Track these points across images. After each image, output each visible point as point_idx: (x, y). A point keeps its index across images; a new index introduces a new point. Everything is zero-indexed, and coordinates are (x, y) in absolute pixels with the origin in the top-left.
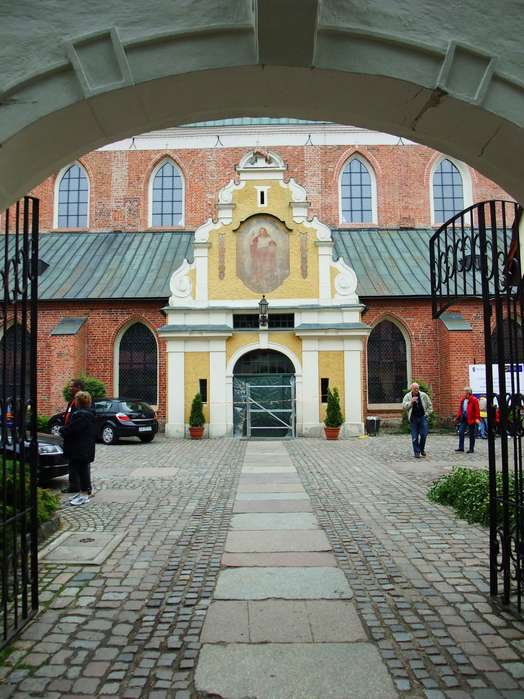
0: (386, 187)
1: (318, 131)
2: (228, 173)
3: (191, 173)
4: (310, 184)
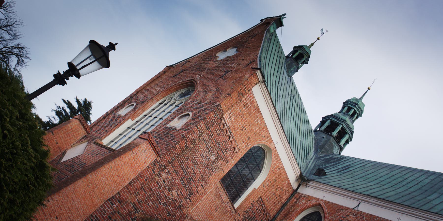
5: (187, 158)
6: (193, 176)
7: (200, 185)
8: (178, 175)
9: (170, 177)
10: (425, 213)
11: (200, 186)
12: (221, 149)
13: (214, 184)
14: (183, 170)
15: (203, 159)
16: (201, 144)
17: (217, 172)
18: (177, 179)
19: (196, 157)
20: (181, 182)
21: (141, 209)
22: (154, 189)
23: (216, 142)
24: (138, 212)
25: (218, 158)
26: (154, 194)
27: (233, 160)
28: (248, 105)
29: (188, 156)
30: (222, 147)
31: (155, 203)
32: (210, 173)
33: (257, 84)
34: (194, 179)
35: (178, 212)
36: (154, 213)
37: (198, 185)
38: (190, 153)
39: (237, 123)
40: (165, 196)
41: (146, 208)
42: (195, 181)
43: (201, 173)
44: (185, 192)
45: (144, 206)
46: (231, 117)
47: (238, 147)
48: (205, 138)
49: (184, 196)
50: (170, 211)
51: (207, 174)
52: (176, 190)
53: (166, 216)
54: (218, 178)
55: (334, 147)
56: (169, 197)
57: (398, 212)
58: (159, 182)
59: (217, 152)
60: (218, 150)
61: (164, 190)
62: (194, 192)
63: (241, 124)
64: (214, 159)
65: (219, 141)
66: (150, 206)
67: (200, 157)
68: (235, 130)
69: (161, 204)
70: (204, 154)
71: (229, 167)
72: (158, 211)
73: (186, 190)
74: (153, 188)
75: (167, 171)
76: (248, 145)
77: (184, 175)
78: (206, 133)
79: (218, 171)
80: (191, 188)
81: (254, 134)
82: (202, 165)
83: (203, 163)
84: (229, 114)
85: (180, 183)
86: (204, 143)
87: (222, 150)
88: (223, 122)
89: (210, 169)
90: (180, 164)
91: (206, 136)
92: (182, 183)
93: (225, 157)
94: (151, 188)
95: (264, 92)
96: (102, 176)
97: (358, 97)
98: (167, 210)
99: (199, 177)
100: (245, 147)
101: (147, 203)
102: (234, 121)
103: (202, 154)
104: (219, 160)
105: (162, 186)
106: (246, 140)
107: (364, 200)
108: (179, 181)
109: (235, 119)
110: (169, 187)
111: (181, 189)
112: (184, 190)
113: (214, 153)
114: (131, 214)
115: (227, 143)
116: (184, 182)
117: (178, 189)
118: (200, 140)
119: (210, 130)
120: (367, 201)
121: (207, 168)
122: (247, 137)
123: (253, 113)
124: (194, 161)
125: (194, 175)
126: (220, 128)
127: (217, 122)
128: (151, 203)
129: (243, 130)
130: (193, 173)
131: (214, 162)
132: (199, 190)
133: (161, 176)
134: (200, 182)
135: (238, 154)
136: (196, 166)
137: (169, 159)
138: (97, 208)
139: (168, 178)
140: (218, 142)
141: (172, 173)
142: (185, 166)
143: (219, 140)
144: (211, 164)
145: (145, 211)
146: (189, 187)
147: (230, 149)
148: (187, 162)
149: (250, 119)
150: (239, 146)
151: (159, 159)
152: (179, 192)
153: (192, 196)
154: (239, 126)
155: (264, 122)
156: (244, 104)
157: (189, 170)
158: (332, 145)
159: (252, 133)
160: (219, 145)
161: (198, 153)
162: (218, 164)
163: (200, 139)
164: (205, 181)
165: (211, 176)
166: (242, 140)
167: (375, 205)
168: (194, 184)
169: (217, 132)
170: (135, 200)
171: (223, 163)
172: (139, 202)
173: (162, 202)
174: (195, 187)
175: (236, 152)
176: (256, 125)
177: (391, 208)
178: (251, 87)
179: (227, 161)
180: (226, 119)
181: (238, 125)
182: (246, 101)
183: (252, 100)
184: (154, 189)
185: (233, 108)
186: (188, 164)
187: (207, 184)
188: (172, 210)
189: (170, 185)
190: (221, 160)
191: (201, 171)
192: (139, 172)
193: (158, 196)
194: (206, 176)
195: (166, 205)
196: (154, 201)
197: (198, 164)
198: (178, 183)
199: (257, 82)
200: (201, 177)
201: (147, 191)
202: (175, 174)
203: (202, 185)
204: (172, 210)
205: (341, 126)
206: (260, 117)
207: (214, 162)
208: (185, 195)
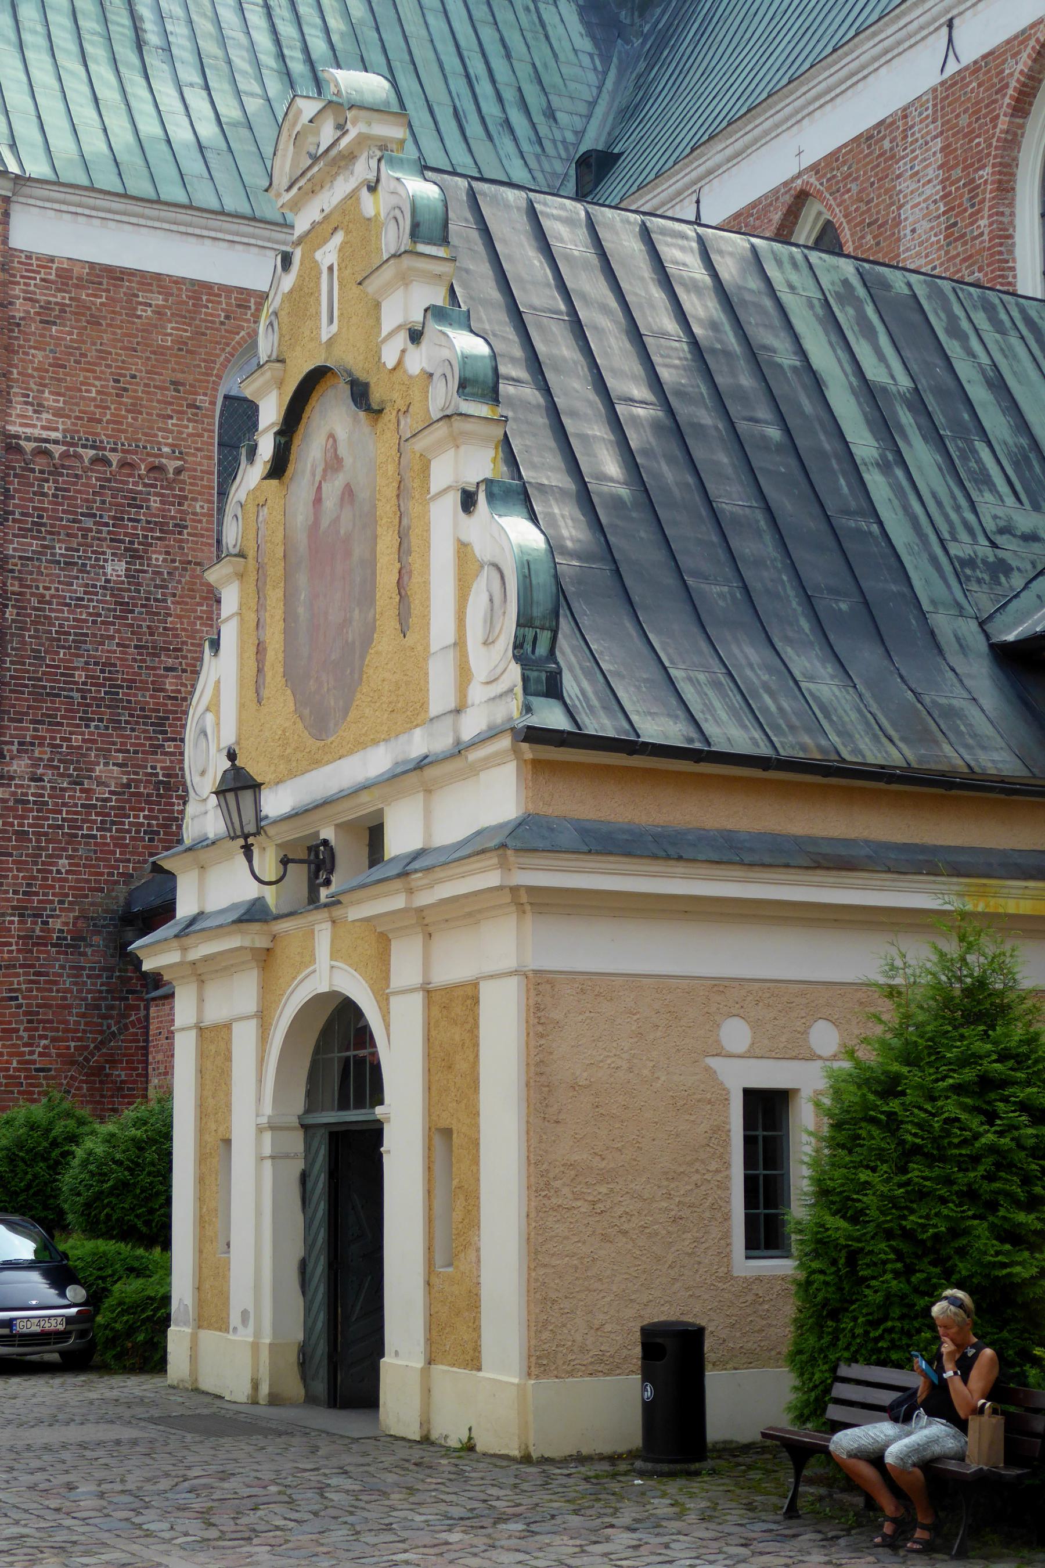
5: (35, 658)
6: (110, 679)
7: (161, 676)
8: (61, 724)
9: (40, 753)
10: (836, 63)
11: (167, 677)
12: (114, 518)
13: (206, 625)
14: (59, 696)
15: (87, 607)
16: (32, 580)
17: (176, 588)
18: (71, 733)
19: (61, 626)
20: (92, 729)
21: (52, 902)
22: (30, 825)
23: (74, 521)
24: (52, 916)
25: (137, 550)
26: (46, 834)
27: (194, 499)
28: (56, 303)
29: (33, 650)
30: (110, 510)
31: (75, 850)
32: (158, 614)
34: (123, 680)
35: (173, 804)
36: (102, 874)
37: (153, 683)
38: (30, 637)
39: (82, 398)
40: (83, 806)
41: (61, 887)
42: (134, 681)
43: (128, 646)
44: (137, 738)
45: (53, 887)
46: (40, 405)
47: (166, 450)
48: (24, 551)
49: (143, 752)
50: (142, 824)
51: (149, 627)
52: (102, 761)
53: (144, 847)
54: (201, 598)
56: (97, 799)
57: (911, 46)
58: (23, 794)
59: (112, 540)
60: (109, 533)
61: (63, 797)
62: (165, 711)
63: (97, 383)
64: (124, 565)
65: (82, 507)
66: (68, 872)
67: (73, 612)
68: (99, 421)
69: (94, 837)
70: (76, 591)
71: (202, 536)
72: (108, 860)
73: (133, 730)
74: (21, 825)
75: (15, 748)
76: (198, 408)
77: (79, 704)
78: (14, 535)
79: (179, 582)
80: (142, 709)
81: (184, 357)
82: (103, 623)
83: (100, 615)
84: (27, 403)
85: (91, 734)
86: (39, 567)
87: (123, 519)
88: (28, 446)
89: (143, 606)
90: (29, 693)
91: (23, 544)
92: (97, 728)
93: (156, 523)
94: (16, 832)
95: (64, 202)
98: (129, 831)
99: (135, 660)
100: (191, 425)
101: (51, 872)
102: (65, 402)
103: (71, 598)
104: (146, 551)
105: (43, 796)
106: (171, 404)
107: (700, 179)
108: (83, 734)
109: (59, 394)
110: (70, 776)
111: (114, 743)
112: (129, 737)
113: (104, 553)
114: (38, 937)
115: (116, 481)
116: (101, 720)
117: (105, 753)
118: (20, 571)
119: (17, 516)
120: (709, 172)
121: (132, 612)
122: (167, 389)
123: (102, 304)
124: (66, 640)
125: (110, 672)
126: (42, 472)
127: (14, 468)
128: (63, 862)
129: (126, 390)
130: (102, 671)
131: (134, 577)
132: (173, 691)
133: (12, 778)
134: (154, 668)
135: (188, 470)
136: (88, 646)
139: (41, 759)
140: (82, 514)
141: (34, 737)
142: (54, 681)
143: (76, 506)
144: (129, 590)
145: (67, 895)
146: (131, 715)
147: (145, 485)
148: (48, 666)
149: (114, 333)
150: (166, 444)
152: (117, 758)
153: (170, 726)
154: (98, 392)
155: (176, 282)
156: (38, 318)
157: (80, 676)
159: (168, 361)
160: (94, 516)
161: (51, 610)
162: (157, 566)
163: (12, 571)
164: (168, 650)
165: (169, 619)
166: (158, 415)
167: (730, 165)
168: (140, 693)
170: (8, 900)
171: (167, 546)
172: (25, 893)
173: (90, 829)
174: (151, 697)
175: (178, 471)
176: (156, 326)
177: (766, 133)
179: (176, 525)
180: (28, 430)
181: (93, 395)
182: (37, 301)
183: (53, 277)
184: (30, 825)
185: (19, 373)
186: (58, 667)
187: (180, 650)
188: (145, 817)
189: (66, 769)
190: (151, 545)
191: (120, 638)
193: (61, 827)
194: (152, 634)
195: (113, 823)
196: (65, 850)
197: (86, 635)
198: (84, 741)
200: (141, 654)
201: (14, 848)
202: (48, 731)
203: (167, 669)
204: (145, 817)
206: (143, 284)
207: (134, 577)
208: (144, 745)
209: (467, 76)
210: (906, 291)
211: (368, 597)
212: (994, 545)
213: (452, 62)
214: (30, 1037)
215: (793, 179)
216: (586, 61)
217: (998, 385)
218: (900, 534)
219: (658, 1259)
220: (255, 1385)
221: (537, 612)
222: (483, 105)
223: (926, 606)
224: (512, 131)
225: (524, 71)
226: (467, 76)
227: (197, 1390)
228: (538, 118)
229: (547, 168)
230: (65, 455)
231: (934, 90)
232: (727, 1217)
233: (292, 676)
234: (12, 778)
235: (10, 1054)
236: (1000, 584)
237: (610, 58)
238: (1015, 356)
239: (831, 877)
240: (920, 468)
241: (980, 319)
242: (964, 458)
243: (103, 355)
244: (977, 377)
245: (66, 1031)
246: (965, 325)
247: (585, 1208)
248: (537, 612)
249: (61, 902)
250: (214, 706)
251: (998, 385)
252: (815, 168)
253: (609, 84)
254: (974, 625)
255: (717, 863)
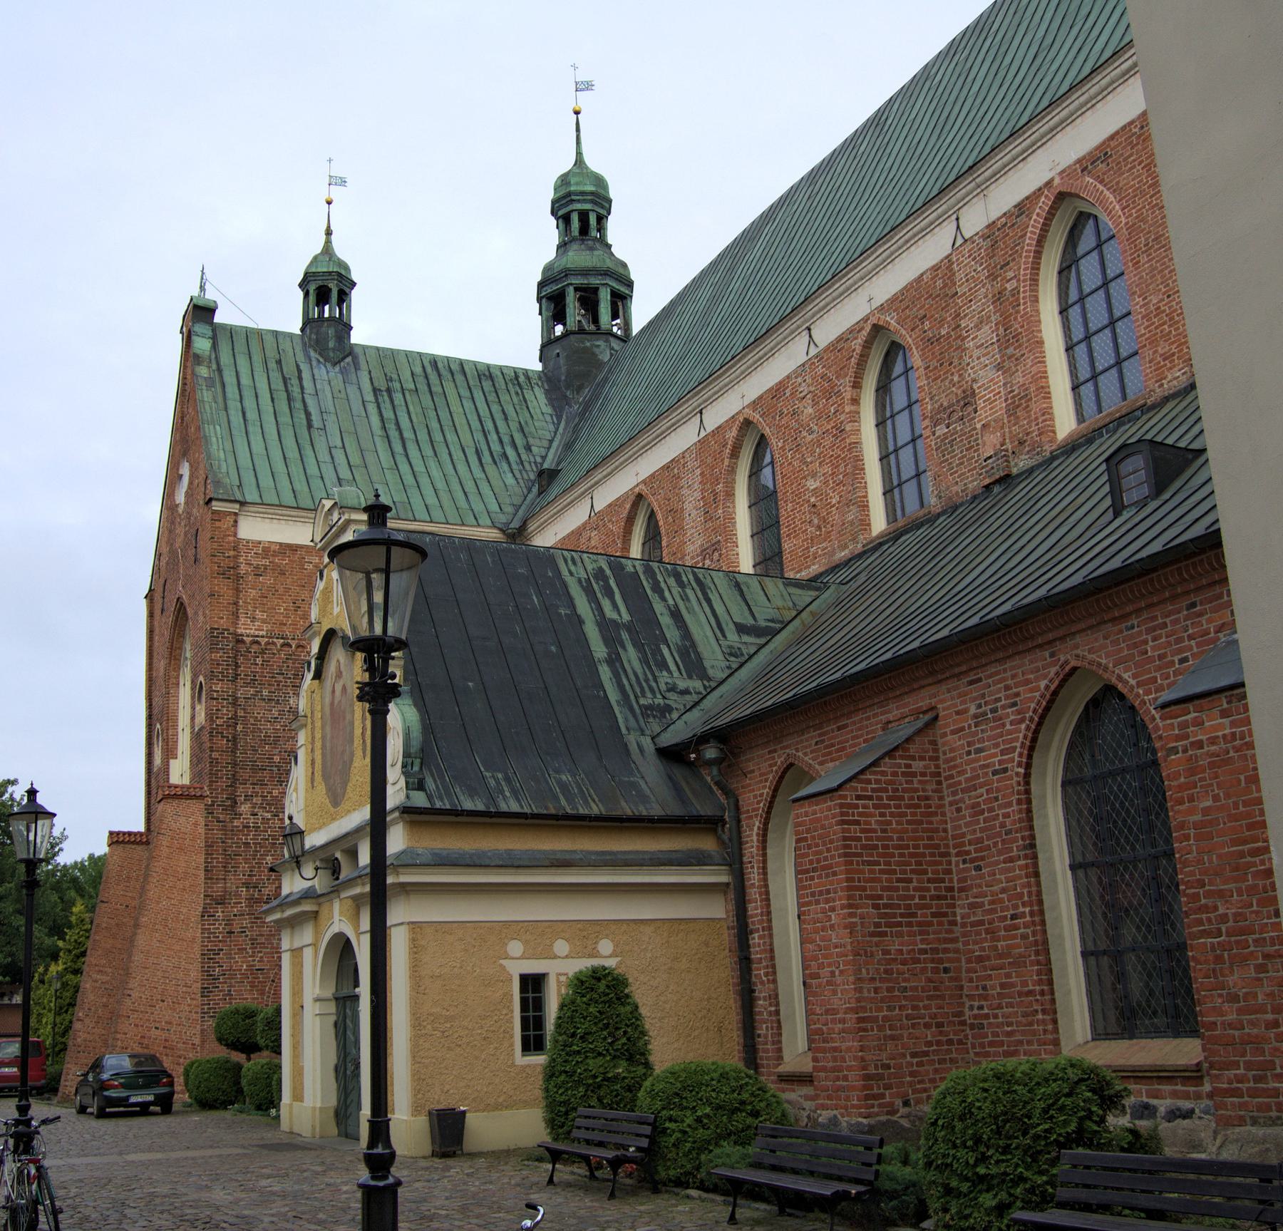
0: (1144, 259)
1: (968, 194)
2: (832, 408)
3: (780, 444)
4: (976, 353)
33: (236, 522)
55: (596, 350)
68: (285, 625)
75: (243, 798)
88: (248, 640)
96: (158, 903)
97: (567, 164)
107: (592, 486)
120: (596, 483)
128: (269, 858)
133: (241, 815)
137: (222, 784)
138: (199, 940)
151: (209, 801)
158: (586, 350)
169: (257, 664)
178: (231, 538)
192: (203, 845)
193: (267, 839)
199: (230, 519)
205: (571, 290)
209: (484, 431)
210: (632, 570)
211: (352, 741)
212: (664, 698)
213: (475, 424)
214: (253, 952)
215: (635, 487)
216: (548, 418)
217: (676, 615)
218: (613, 696)
219: (477, 1058)
220: (313, 1127)
221: (413, 750)
222: (491, 445)
223: (624, 731)
224: (507, 458)
225: (514, 426)
226: (484, 431)
227: (292, 1133)
228: (522, 451)
229: (526, 477)
230: (268, 643)
231: (695, 444)
232: (512, 1036)
233: (326, 777)
234: (241, 815)
235: (243, 962)
236: (665, 717)
237: (561, 416)
238: (688, 600)
239: (560, 871)
240: (629, 661)
241: (672, 581)
242: (653, 654)
243: (287, 590)
244: (666, 611)
245: (272, 948)
246: (663, 585)
247: (439, 1034)
248: (413, 750)
249: (268, 879)
250: (296, 790)
251: (676, 615)
252: (644, 482)
253: (561, 430)
254: (649, 740)
255: (501, 866)
